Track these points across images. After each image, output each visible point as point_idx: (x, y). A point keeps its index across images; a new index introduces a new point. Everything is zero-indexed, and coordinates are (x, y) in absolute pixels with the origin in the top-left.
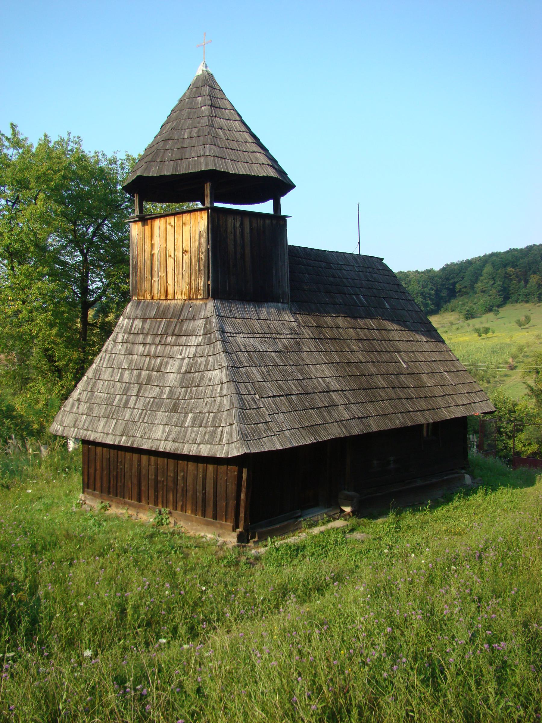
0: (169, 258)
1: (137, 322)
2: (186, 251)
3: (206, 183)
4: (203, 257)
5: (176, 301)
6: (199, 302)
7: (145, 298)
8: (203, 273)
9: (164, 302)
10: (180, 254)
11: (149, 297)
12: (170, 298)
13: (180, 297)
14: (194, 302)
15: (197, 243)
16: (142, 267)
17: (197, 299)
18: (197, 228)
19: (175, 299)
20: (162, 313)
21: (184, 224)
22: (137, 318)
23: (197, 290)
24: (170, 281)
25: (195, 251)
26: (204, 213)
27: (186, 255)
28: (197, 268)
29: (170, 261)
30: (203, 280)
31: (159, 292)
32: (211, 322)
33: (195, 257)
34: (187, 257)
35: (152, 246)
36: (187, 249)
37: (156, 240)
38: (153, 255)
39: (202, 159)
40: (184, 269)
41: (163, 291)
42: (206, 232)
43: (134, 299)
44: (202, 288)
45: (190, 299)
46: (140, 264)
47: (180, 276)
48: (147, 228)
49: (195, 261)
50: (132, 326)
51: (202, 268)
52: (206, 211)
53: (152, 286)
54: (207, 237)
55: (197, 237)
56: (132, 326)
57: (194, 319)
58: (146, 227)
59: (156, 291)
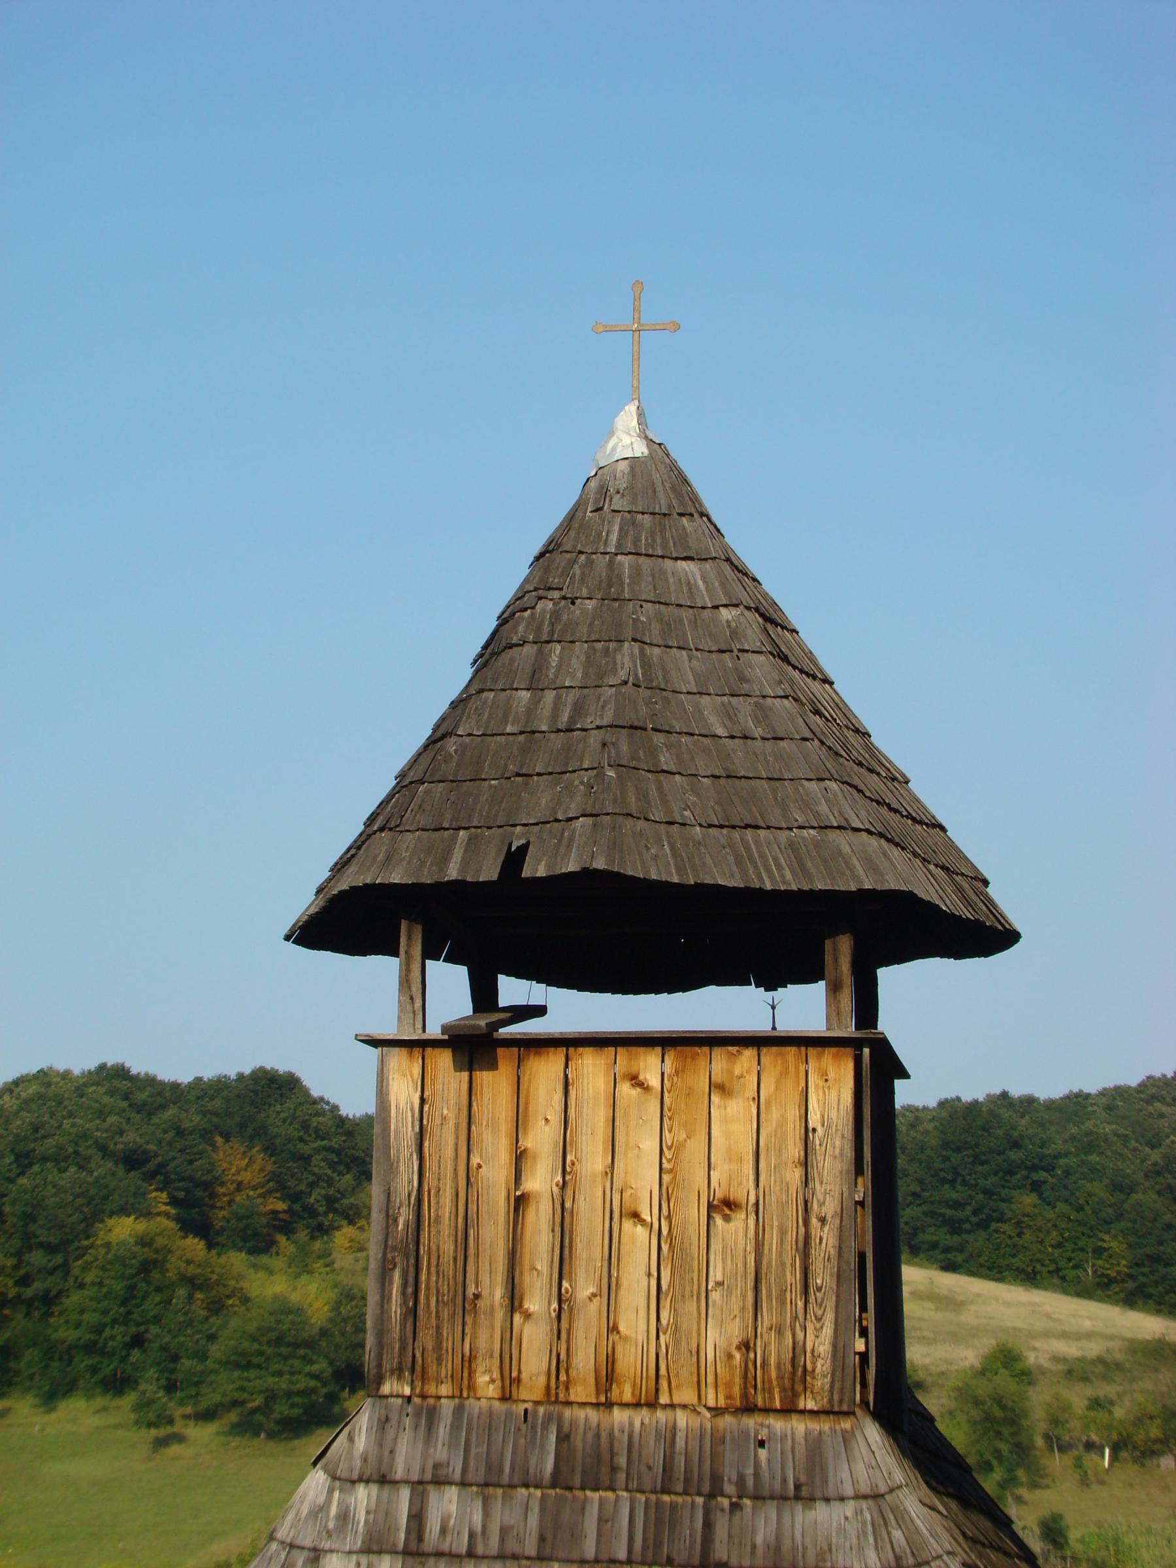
0: (628, 1225)
1: (447, 1504)
2: (728, 1205)
3: (835, 933)
4: (826, 1238)
5: (660, 1415)
6: (799, 1426)
7: (465, 1385)
8: (830, 1304)
9: (593, 1415)
10: (692, 1213)
11: (486, 1383)
12: (627, 1397)
13: (687, 1395)
14: (778, 1424)
15: (795, 1176)
16: (448, 1247)
17: (789, 1410)
18: (793, 1114)
19: (653, 1405)
20: (588, 1467)
21: (720, 1088)
22: (439, 1482)
23: (797, 1376)
24: (634, 1321)
25: (783, 1206)
26: (836, 1057)
27: (727, 1219)
28: (793, 1278)
29: (637, 1238)
30: (828, 1330)
31: (560, 1365)
32: (901, 1517)
33: (783, 1232)
34: (735, 1231)
35: (520, 1158)
36: (738, 1194)
37: (542, 1138)
38: (520, 1203)
39: (842, 840)
40: (716, 1274)
41: (584, 1360)
42: (849, 1132)
43: (386, 1389)
44: (823, 1366)
45: (749, 1408)
46: (441, 1239)
47: (691, 1306)
48: (495, 1085)
49: (780, 1250)
50: (417, 1518)
51: (822, 1276)
52: (850, 1051)
53: (510, 1337)
54: (849, 1153)
55: (794, 1150)
56: (417, 1518)
57: (804, 1494)
58: (484, 1077)
59: (534, 1364)
